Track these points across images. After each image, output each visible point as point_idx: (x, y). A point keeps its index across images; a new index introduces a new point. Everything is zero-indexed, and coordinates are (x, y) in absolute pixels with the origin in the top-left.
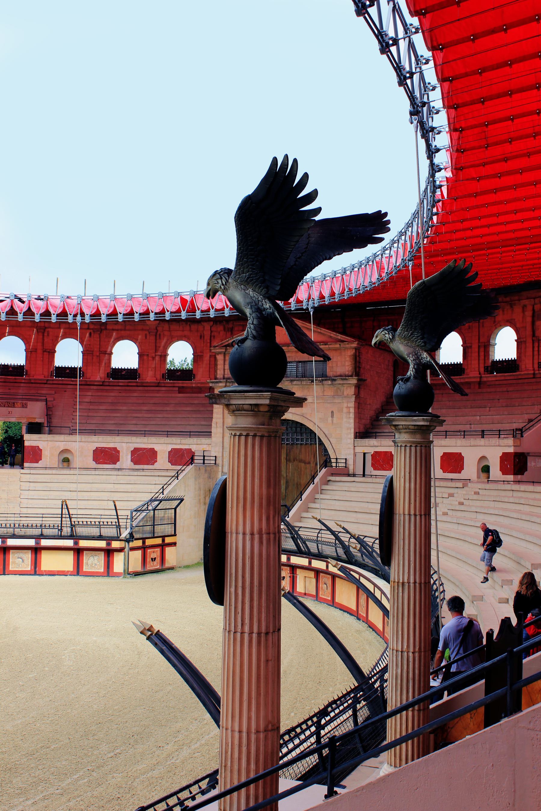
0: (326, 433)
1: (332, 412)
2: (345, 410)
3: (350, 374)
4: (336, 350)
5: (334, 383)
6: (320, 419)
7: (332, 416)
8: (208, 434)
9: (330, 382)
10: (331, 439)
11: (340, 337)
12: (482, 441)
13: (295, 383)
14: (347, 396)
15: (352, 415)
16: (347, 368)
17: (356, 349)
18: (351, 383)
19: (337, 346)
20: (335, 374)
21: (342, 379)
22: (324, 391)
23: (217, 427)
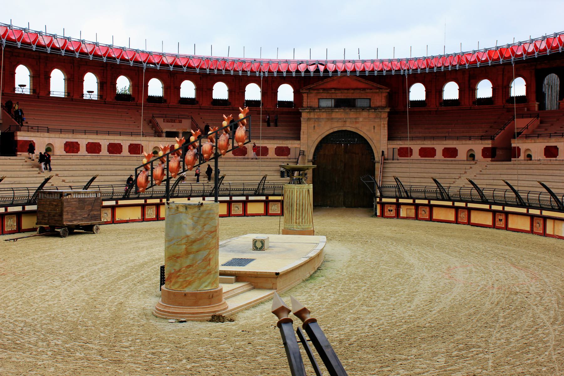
0: (371, 137)
1: (374, 127)
2: (382, 125)
3: (385, 106)
4: (376, 93)
5: (376, 111)
6: (367, 130)
7: (374, 129)
8: (298, 138)
9: (373, 110)
10: (374, 141)
11: (379, 86)
12: (470, 142)
13: (352, 110)
14: (384, 118)
15: (386, 128)
16: (383, 103)
17: (389, 93)
18: (386, 111)
19: (378, 91)
20: (375, 106)
21: (382, 109)
22: (369, 115)
23: (304, 134)
